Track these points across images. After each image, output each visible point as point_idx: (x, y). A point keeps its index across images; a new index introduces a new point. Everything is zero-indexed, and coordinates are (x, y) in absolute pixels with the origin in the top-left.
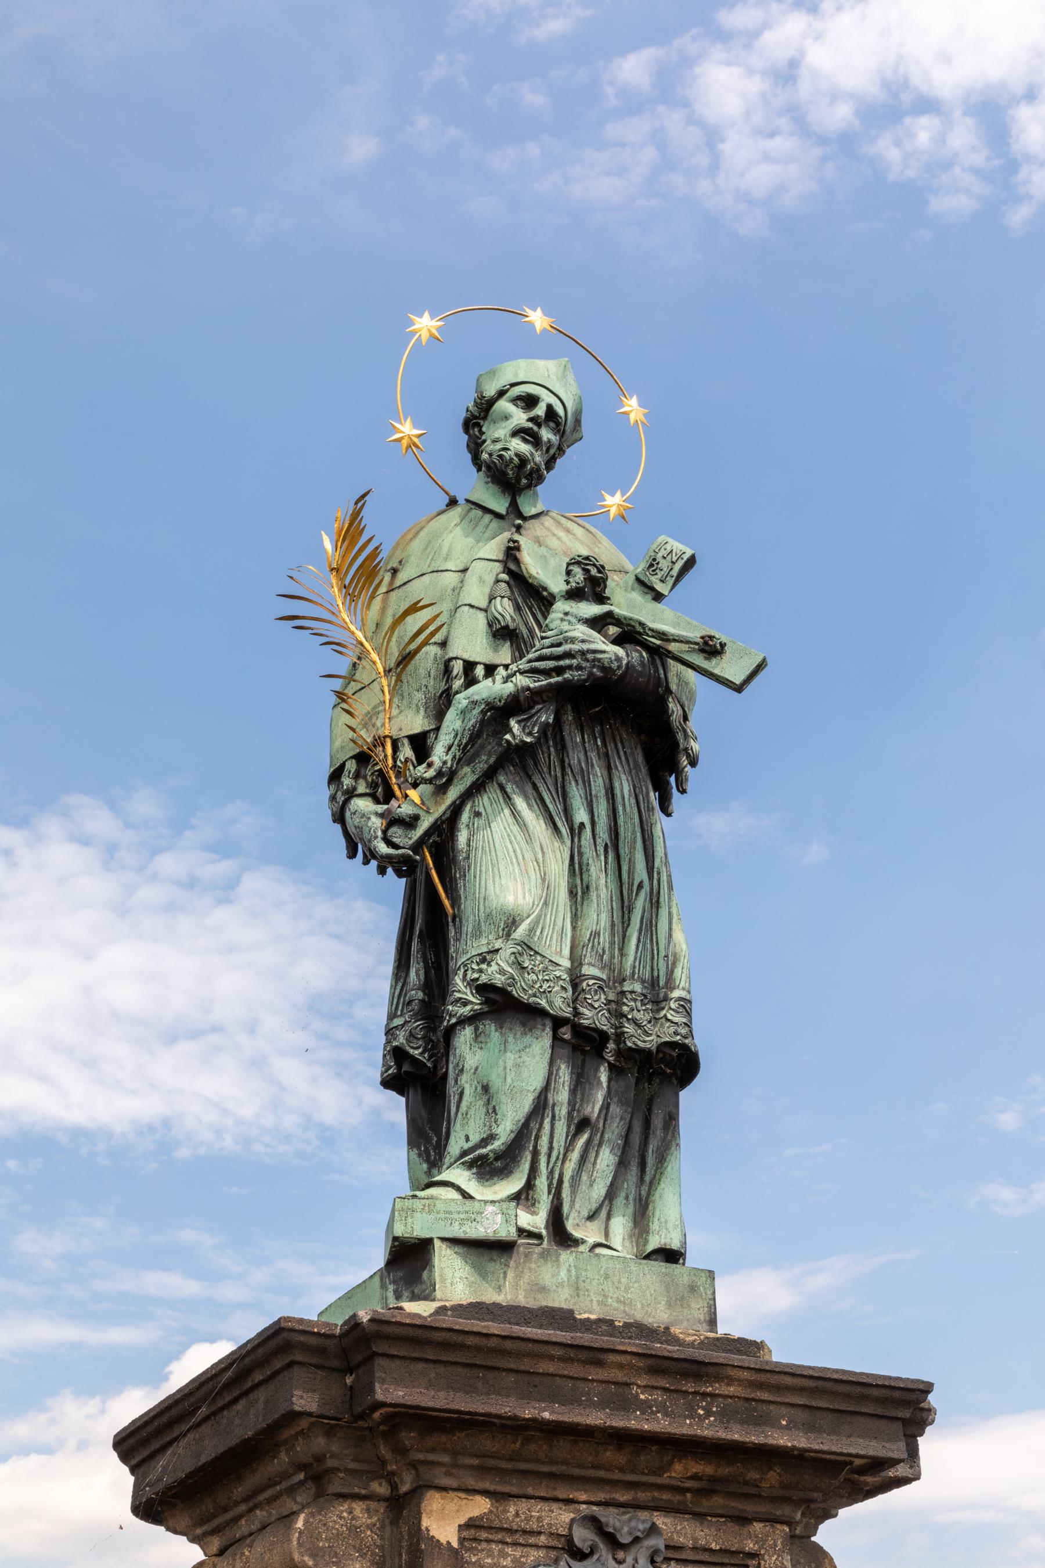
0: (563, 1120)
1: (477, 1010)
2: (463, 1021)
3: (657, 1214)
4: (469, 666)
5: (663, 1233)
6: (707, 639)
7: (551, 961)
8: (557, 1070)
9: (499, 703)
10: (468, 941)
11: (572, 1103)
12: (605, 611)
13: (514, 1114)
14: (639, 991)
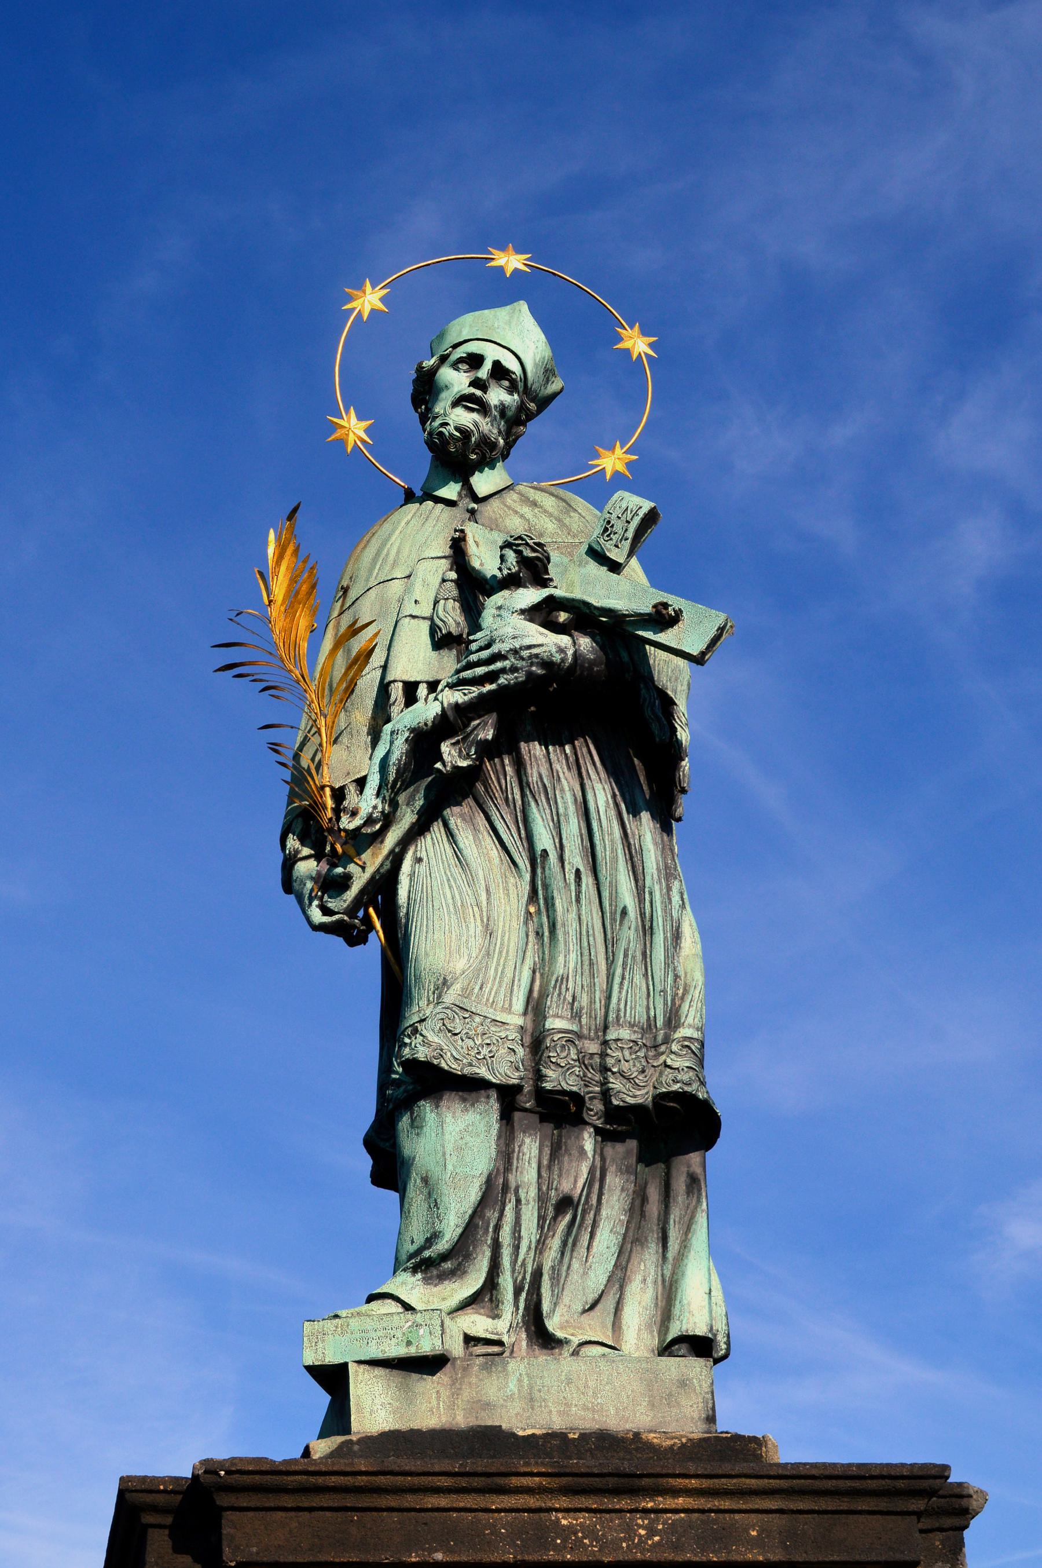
0: (532, 1203)
6: (660, 607)
8: (520, 1147)
9: (424, 727)
12: (544, 596)
13: (458, 1205)
14: (627, 1037)
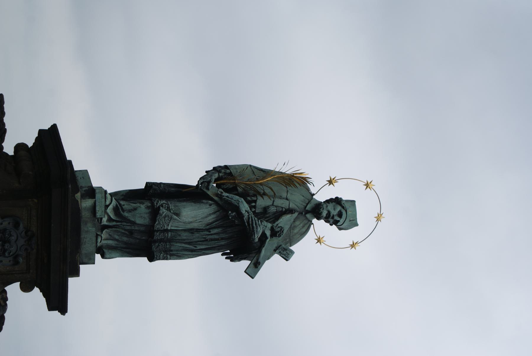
2: (152, 204)
4: (255, 201)
5: (108, 253)
7: (169, 224)
11: (136, 230)
14: (167, 247)
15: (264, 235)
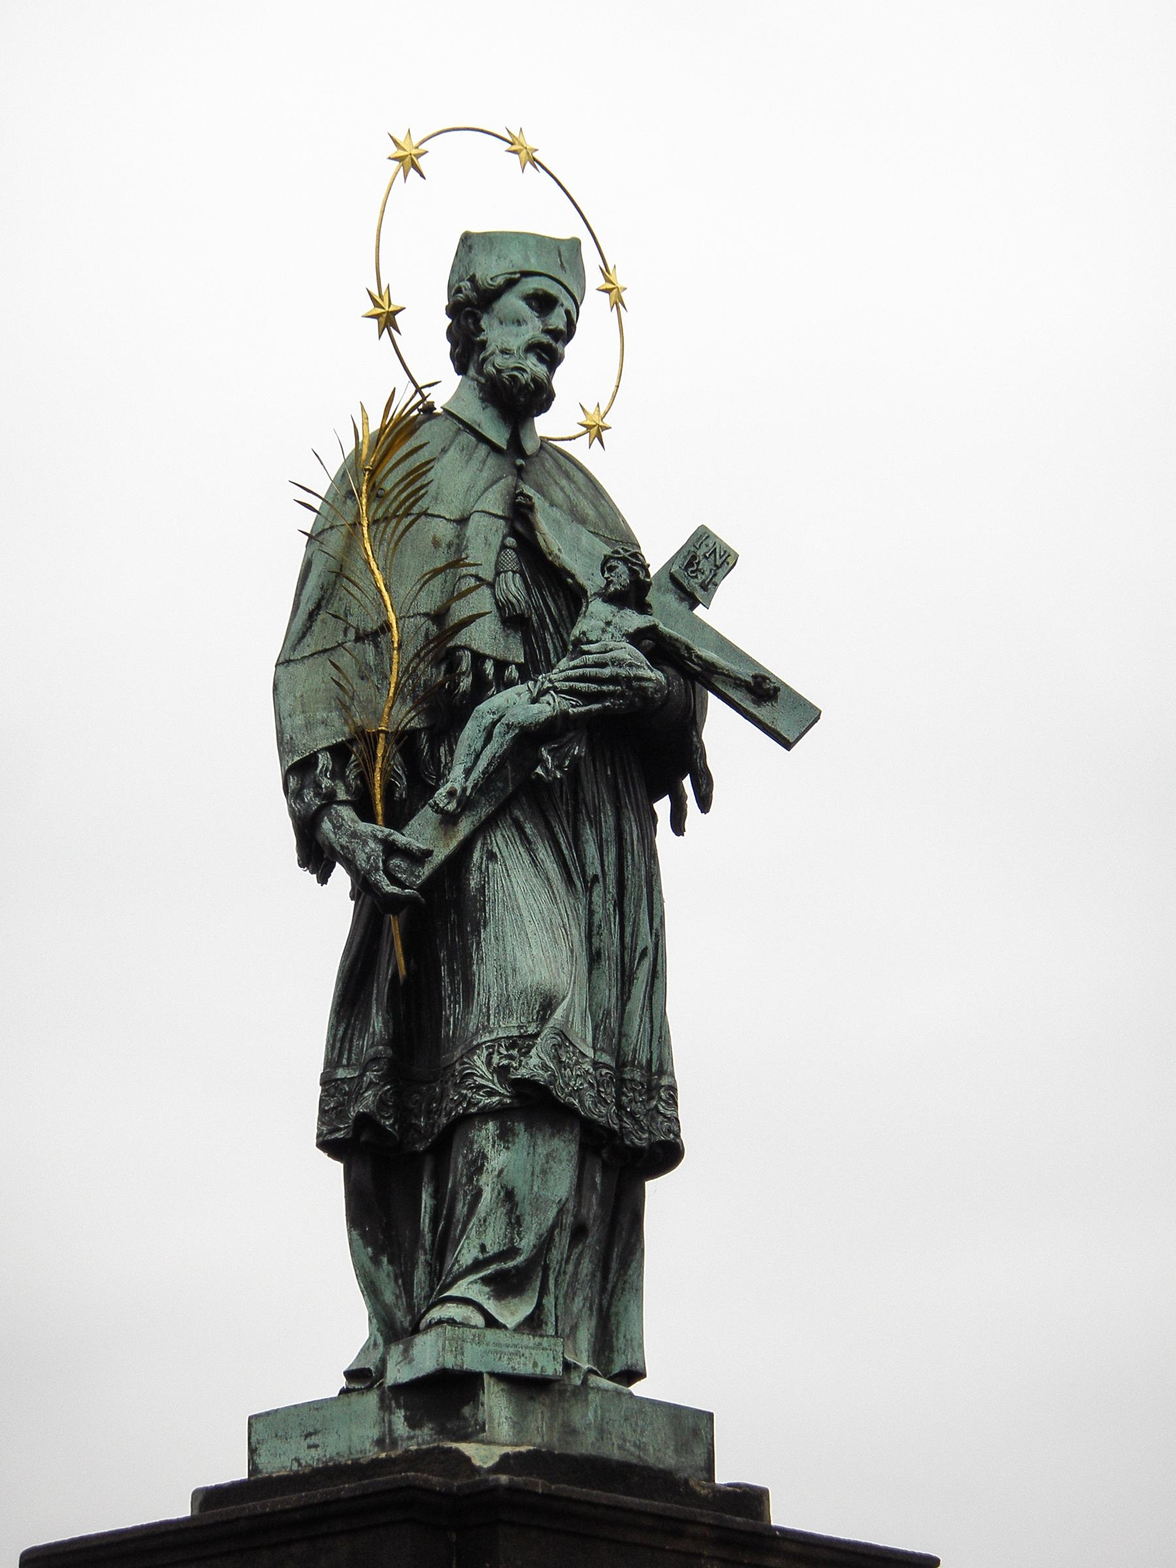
0: (568, 1230)
1: (506, 1104)
2: (487, 1114)
3: (622, 1329)
4: (479, 658)
7: (580, 1052)
10: (492, 1017)
15: (636, 638)
